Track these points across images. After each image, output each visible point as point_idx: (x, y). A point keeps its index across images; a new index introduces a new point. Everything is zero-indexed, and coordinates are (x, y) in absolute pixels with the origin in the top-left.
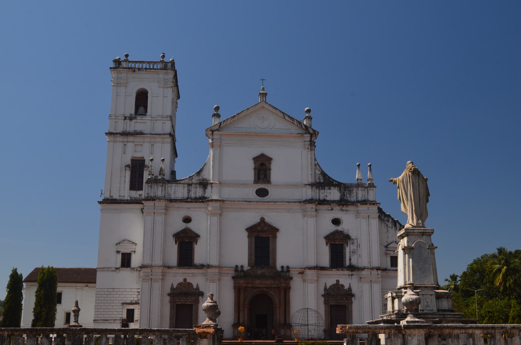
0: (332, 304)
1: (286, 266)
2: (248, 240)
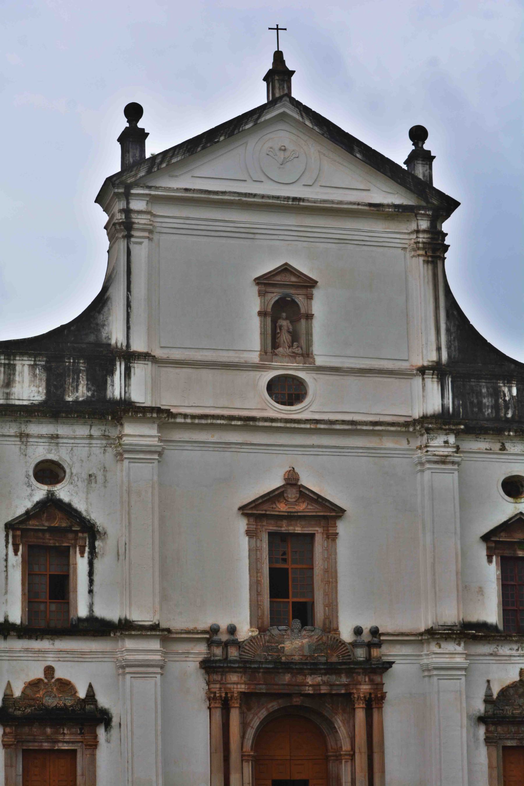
0: (509, 743)
1: (369, 628)
2: (249, 542)
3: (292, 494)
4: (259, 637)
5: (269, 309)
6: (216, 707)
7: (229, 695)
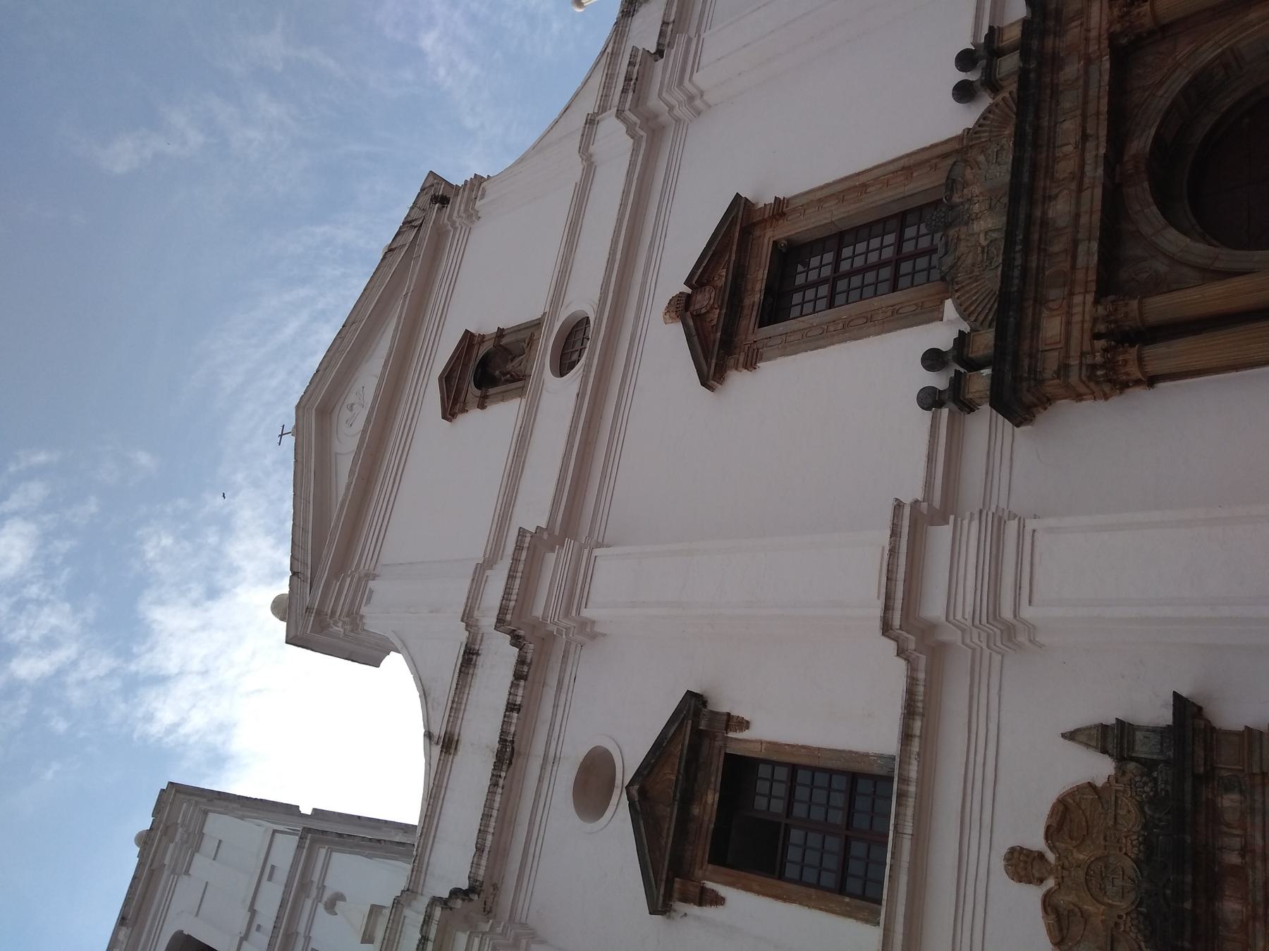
2: (769, 359)
3: (704, 300)
4: (957, 295)
5: (478, 392)
6: (1140, 360)
7: (1102, 328)
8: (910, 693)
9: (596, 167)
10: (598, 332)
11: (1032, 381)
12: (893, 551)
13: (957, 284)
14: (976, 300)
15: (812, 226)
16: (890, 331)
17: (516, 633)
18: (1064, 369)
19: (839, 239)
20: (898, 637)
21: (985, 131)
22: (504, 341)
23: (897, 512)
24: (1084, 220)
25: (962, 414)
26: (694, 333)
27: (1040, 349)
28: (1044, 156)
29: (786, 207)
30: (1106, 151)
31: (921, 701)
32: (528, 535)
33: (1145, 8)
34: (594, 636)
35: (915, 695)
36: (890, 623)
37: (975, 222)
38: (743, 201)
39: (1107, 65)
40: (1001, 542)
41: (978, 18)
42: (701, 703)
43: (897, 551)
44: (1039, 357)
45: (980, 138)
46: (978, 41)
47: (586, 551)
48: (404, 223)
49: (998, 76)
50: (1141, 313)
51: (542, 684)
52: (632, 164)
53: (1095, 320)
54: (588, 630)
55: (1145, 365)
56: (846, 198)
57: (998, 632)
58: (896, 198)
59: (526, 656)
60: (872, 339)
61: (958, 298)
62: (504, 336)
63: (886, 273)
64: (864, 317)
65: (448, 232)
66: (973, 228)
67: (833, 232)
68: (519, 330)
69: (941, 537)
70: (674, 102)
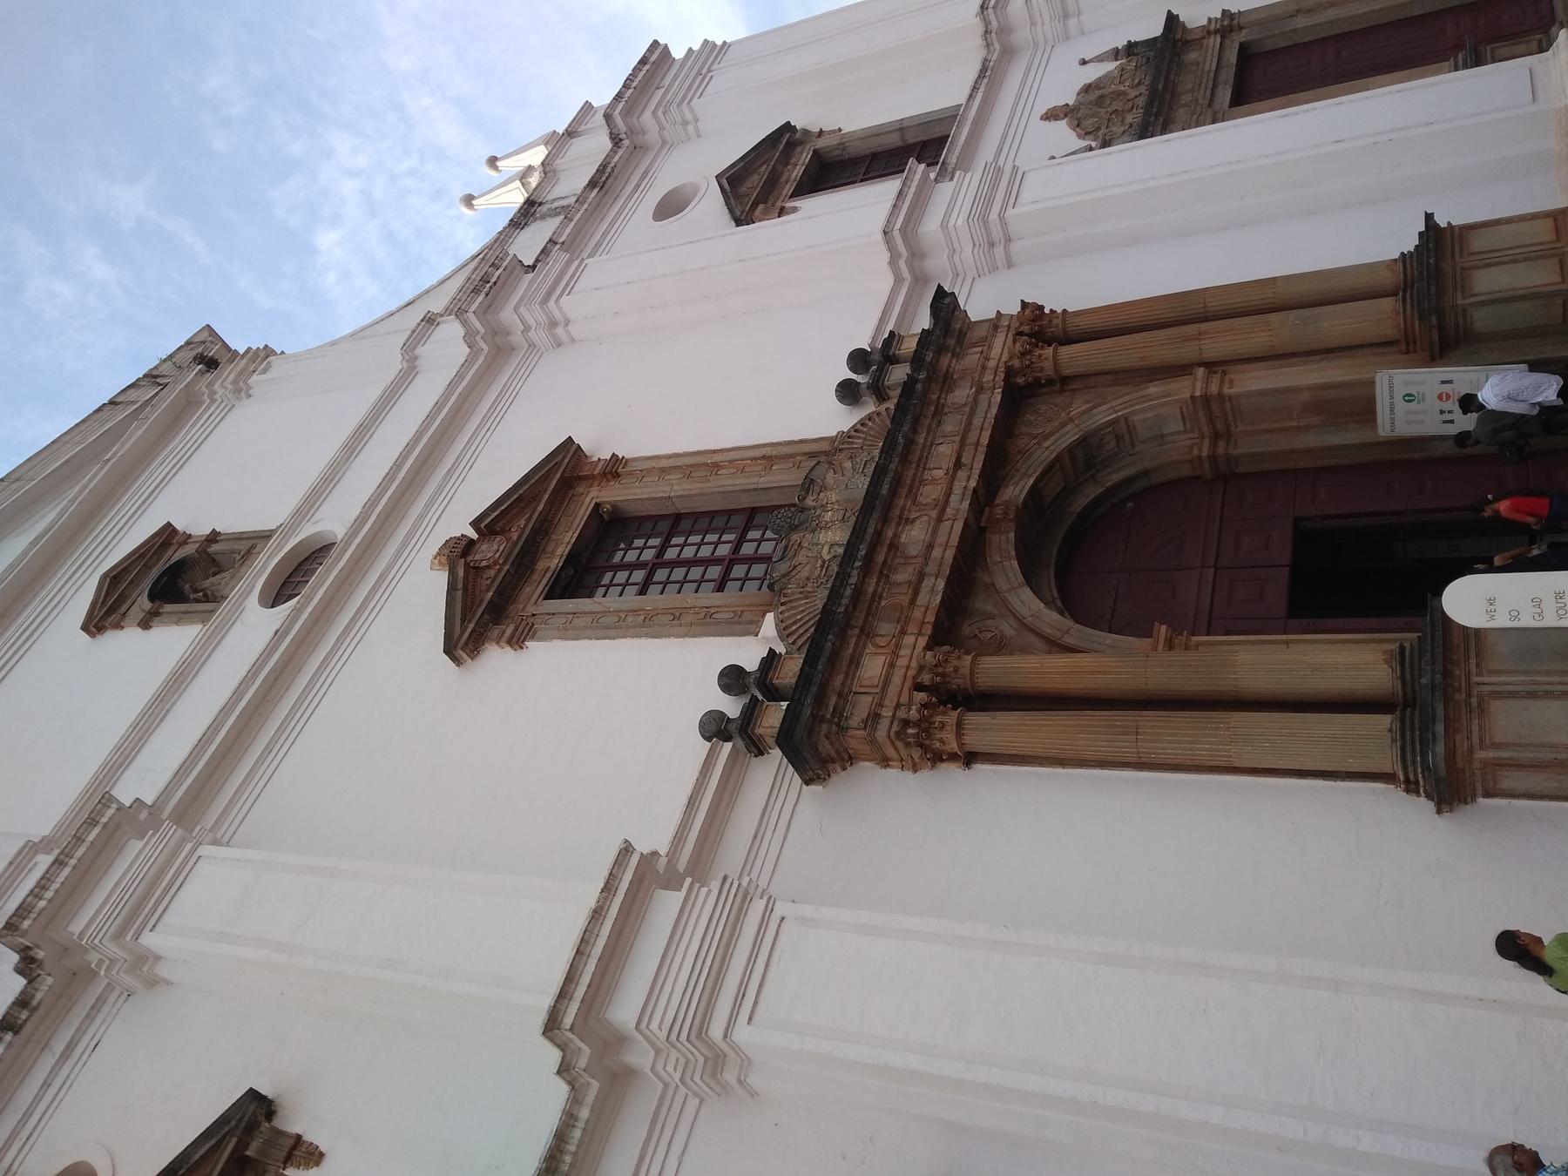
2: (542, 639)
4: (782, 608)
5: (147, 605)
6: (959, 726)
7: (926, 678)
8: (560, 1137)
9: (417, 372)
10: (338, 560)
11: (834, 726)
12: (597, 914)
13: (784, 596)
14: (801, 619)
15: (646, 496)
16: (694, 636)
17: (32, 953)
18: (874, 717)
19: (675, 522)
20: (566, 1045)
21: (860, 438)
22: (214, 548)
23: (621, 858)
24: (936, 553)
25: (749, 755)
26: (460, 585)
27: (854, 690)
28: (911, 473)
29: (622, 468)
30: (978, 482)
31: (571, 1153)
32: (114, 806)
33: (1047, 351)
34: (153, 983)
35: (567, 1143)
36: (559, 1019)
37: (823, 531)
38: (574, 447)
39: (998, 398)
40: (739, 926)
41: (882, 321)
42: (264, 1111)
43: (603, 914)
44: (850, 699)
45: (852, 443)
46: (876, 346)
47: (189, 846)
48: (145, 376)
49: (886, 383)
50: (972, 671)
51: (42, 1046)
52: (459, 376)
53: (921, 668)
54: (145, 969)
55: (963, 734)
56: (693, 474)
57: (701, 1060)
58: (746, 487)
59: (33, 995)
60: (672, 640)
61: (781, 613)
62: (216, 541)
63: (715, 572)
64: (672, 614)
65: (204, 402)
66: (819, 538)
67: (669, 512)
68: (240, 539)
69: (667, 904)
70: (532, 322)
